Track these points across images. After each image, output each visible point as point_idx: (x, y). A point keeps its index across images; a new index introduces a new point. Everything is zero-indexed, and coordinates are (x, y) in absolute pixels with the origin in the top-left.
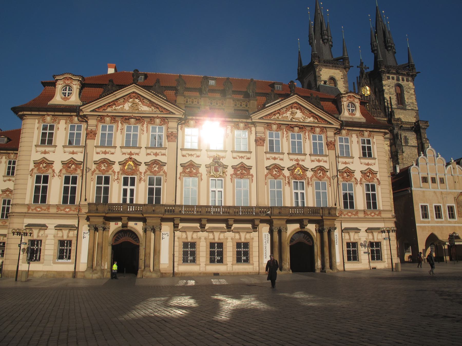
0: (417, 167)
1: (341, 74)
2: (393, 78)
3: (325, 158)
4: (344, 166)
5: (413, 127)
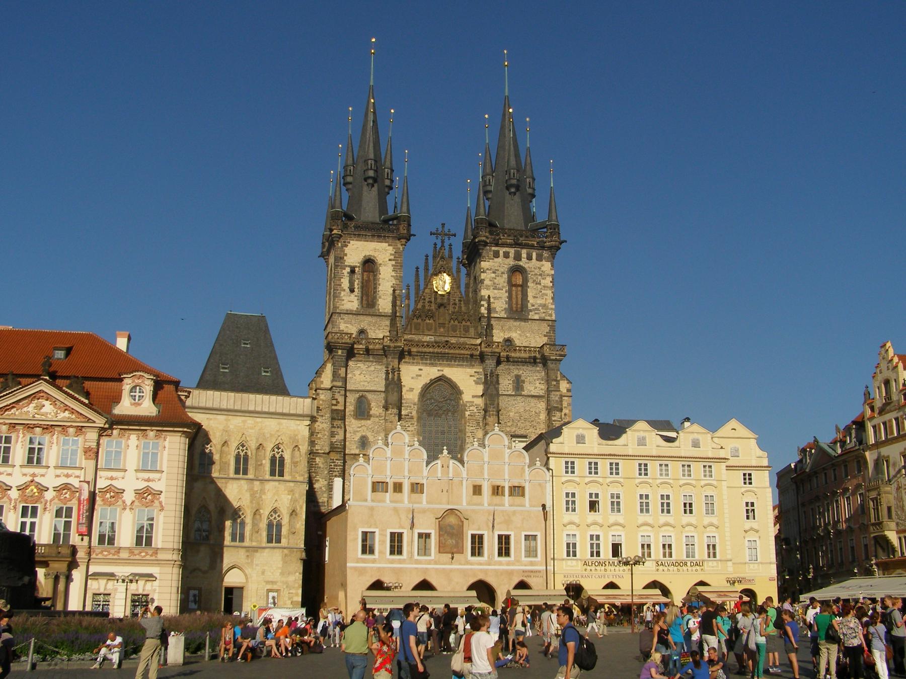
0: (366, 464)
1: (391, 250)
2: (506, 255)
3: (77, 472)
4: (109, 482)
5: (535, 358)
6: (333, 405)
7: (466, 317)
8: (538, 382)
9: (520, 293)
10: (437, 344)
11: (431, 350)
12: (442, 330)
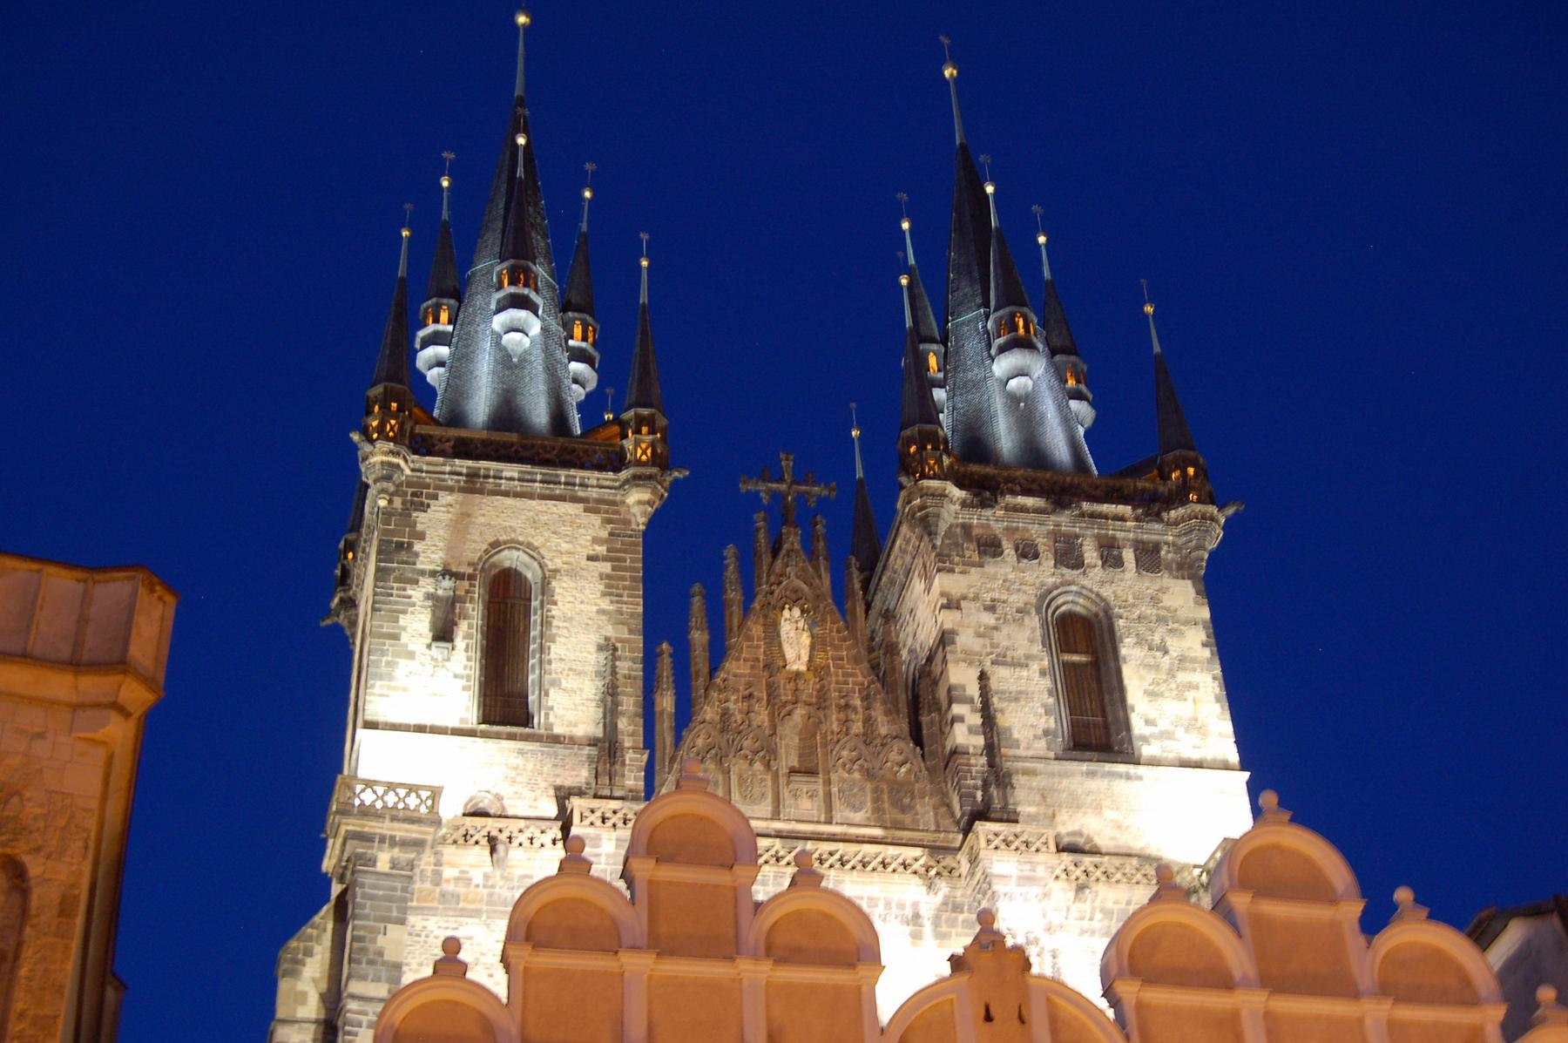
2: (1027, 552)
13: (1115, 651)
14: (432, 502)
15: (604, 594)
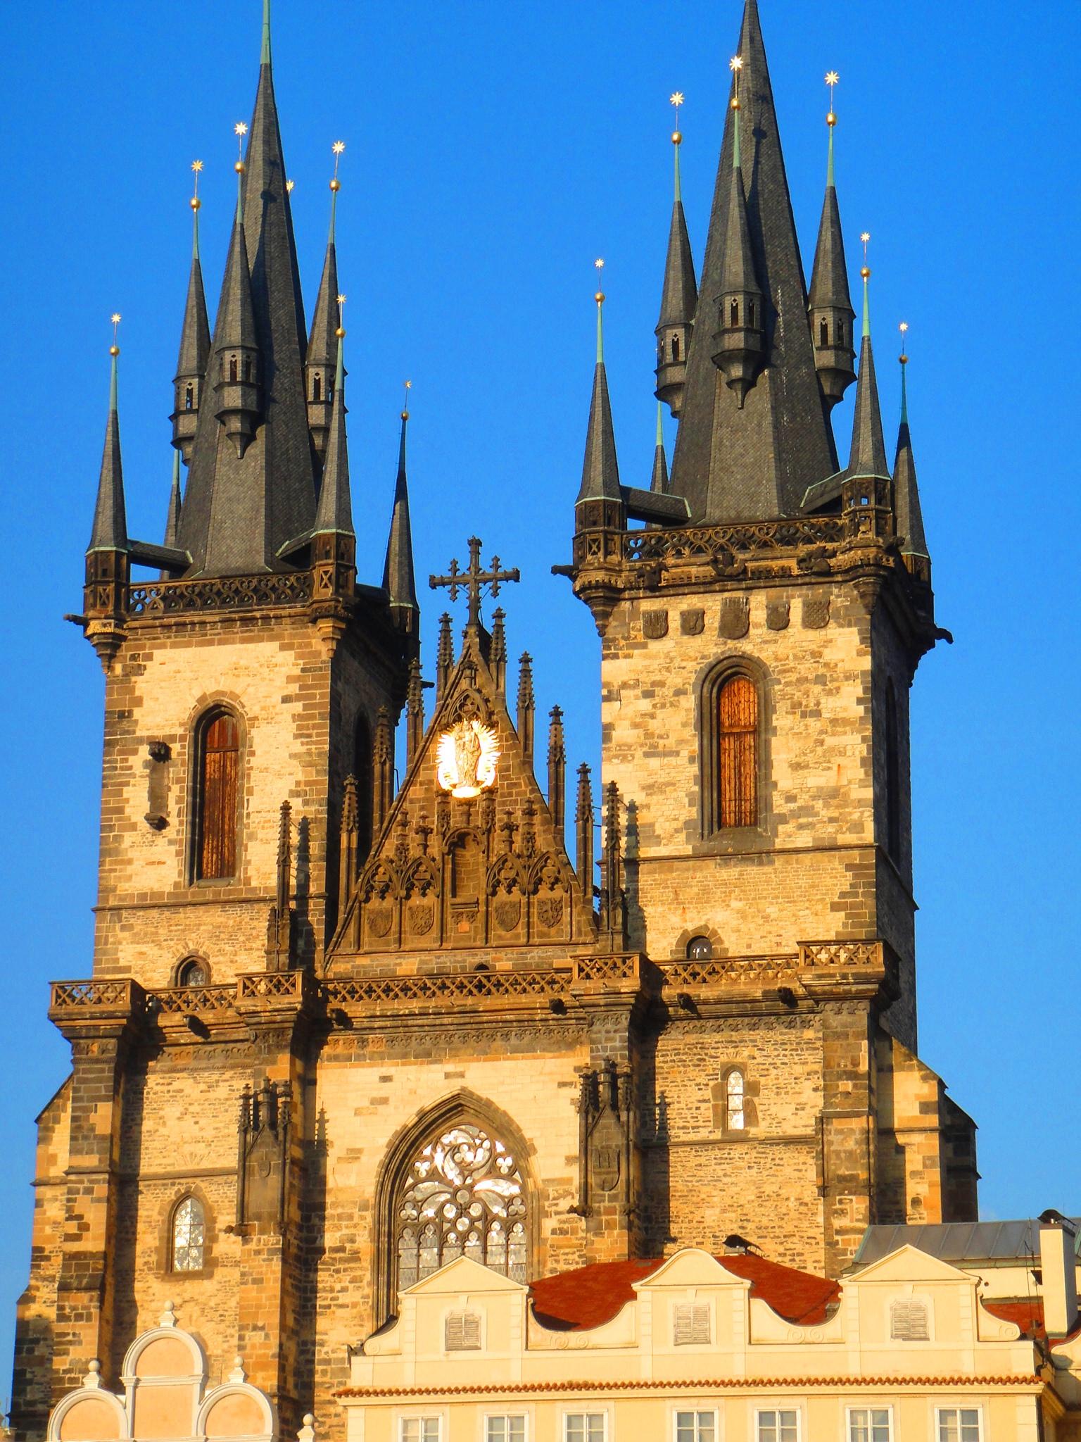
2: (693, 624)
6: (69, 1238)
7: (549, 870)
8: (809, 1085)
9: (749, 756)
10: (439, 982)
11: (415, 1005)
12: (465, 926)
13: (768, 721)
14: (148, 664)
15: (296, 737)
